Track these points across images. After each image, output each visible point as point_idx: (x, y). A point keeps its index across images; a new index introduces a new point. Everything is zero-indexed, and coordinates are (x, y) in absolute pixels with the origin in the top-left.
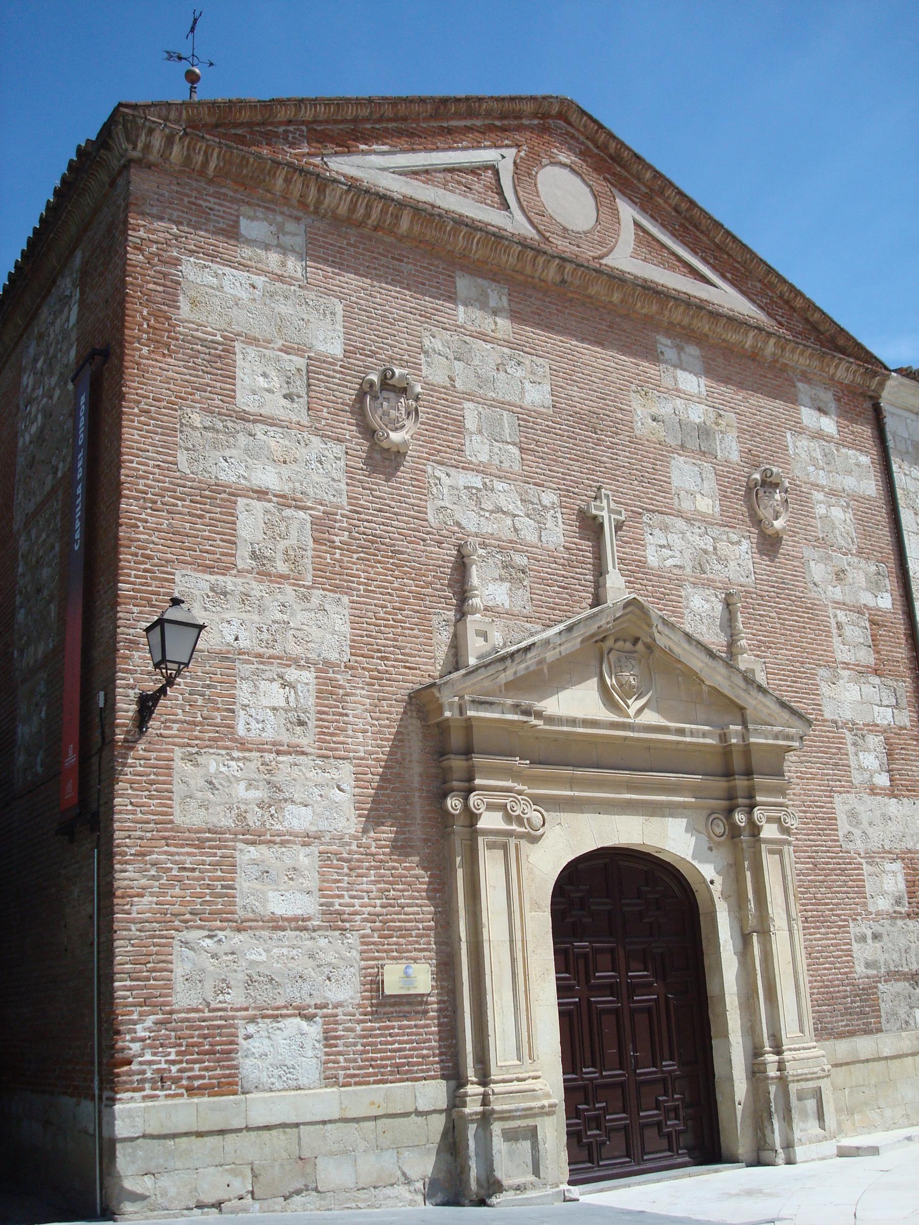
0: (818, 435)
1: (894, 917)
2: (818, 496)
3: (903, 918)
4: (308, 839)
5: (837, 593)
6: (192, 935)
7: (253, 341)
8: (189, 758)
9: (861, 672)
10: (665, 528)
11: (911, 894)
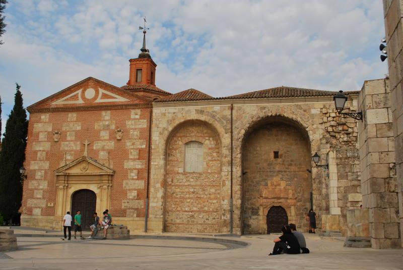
0: (135, 119)
1: (132, 199)
4: (42, 189)
5: (132, 147)
7: (41, 132)
9: (134, 160)
10: (97, 143)
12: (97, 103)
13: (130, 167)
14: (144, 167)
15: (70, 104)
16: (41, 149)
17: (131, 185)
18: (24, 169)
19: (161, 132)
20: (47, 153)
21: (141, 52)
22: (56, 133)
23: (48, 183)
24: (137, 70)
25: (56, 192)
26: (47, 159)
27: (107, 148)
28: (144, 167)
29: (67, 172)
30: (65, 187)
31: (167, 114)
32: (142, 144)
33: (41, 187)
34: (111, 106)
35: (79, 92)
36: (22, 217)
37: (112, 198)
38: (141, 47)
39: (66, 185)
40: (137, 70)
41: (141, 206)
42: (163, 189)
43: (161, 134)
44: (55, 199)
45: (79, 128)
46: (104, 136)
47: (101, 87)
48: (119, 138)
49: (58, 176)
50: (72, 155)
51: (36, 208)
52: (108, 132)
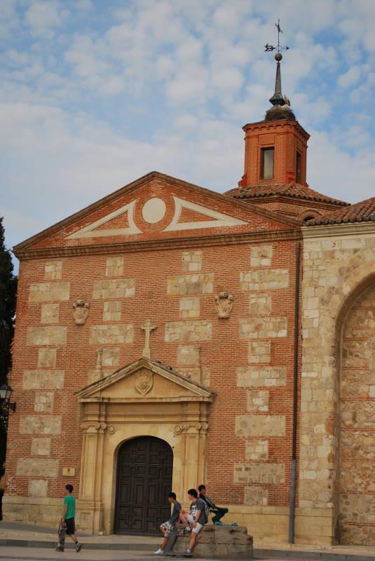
0: (261, 268)
1: (258, 462)
2: (252, 296)
3: (264, 462)
4: (49, 436)
5: (255, 335)
6: (21, 459)
7: (46, 303)
8: (24, 417)
9: (260, 366)
10: (174, 327)
11: (271, 452)
12: (172, 232)
13: (250, 384)
14: (285, 385)
15: (110, 237)
16: (47, 342)
17: (254, 426)
18: (9, 389)
19: (325, 298)
20: (59, 352)
21: (270, 106)
22: (78, 305)
23: (63, 420)
24: (263, 149)
25: (80, 441)
26: (60, 366)
27: (194, 337)
28: (283, 383)
29: (106, 394)
30: (101, 431)
31: (338, 255)
32: (278, 329)
33: (47, 431)
34: (201, 238)
35: (130, 207)
36: (5, 499)
37: (208, 456)
38: (271, 94)
39: (104, 426)
40: (263, 149)
41: (279, 478)
42: (331, 437)
43: (323, 301)
44: (79, 458)
45: (130, 292)
46: (188, 311)
47: (179, 195)
48: (223, 314)
49: (84, 404)
50: (115, 357)
51: (38, 478)
52: (197, 300)
